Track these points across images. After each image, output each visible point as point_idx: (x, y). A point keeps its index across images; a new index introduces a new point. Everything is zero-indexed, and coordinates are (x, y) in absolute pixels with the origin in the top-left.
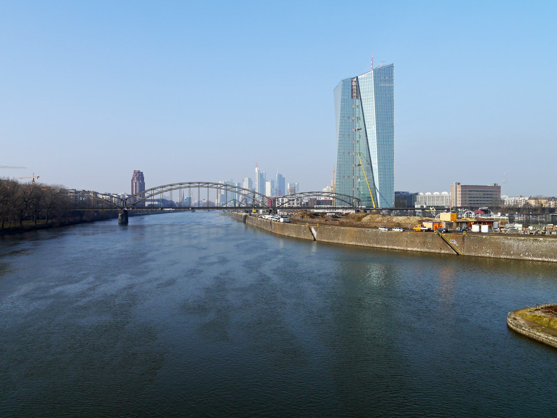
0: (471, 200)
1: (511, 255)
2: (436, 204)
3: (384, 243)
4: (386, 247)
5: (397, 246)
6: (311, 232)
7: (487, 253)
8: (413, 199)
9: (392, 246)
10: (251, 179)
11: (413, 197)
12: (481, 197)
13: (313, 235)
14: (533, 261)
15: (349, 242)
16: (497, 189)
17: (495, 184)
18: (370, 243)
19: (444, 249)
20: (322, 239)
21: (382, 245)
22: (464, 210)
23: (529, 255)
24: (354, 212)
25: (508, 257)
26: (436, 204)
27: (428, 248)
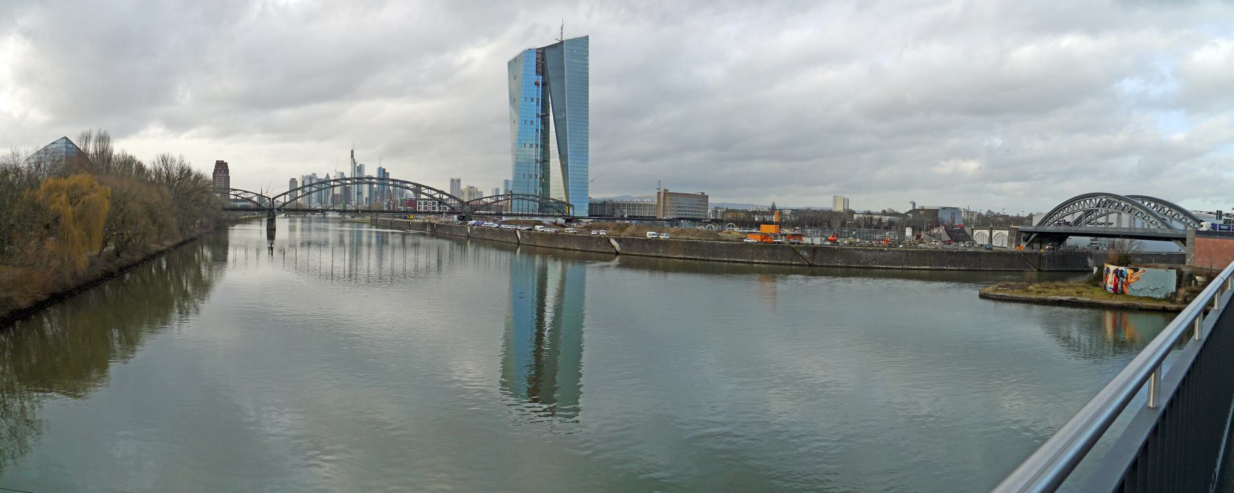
0: (679, 211)
1: (860, 264)
4: (726, 259)
6: (611, 243)
7: (839, 263)
12: (689, 207)
13: (613, 246)
14: (879, 268)
15: (677, 254)
16: (704, 198)
17: (703, 193)
18: (705, 256)
19: (795, 261)
23: (875, 264)
24: (563, 221)
25: (858, 266)
27: (779, 260)
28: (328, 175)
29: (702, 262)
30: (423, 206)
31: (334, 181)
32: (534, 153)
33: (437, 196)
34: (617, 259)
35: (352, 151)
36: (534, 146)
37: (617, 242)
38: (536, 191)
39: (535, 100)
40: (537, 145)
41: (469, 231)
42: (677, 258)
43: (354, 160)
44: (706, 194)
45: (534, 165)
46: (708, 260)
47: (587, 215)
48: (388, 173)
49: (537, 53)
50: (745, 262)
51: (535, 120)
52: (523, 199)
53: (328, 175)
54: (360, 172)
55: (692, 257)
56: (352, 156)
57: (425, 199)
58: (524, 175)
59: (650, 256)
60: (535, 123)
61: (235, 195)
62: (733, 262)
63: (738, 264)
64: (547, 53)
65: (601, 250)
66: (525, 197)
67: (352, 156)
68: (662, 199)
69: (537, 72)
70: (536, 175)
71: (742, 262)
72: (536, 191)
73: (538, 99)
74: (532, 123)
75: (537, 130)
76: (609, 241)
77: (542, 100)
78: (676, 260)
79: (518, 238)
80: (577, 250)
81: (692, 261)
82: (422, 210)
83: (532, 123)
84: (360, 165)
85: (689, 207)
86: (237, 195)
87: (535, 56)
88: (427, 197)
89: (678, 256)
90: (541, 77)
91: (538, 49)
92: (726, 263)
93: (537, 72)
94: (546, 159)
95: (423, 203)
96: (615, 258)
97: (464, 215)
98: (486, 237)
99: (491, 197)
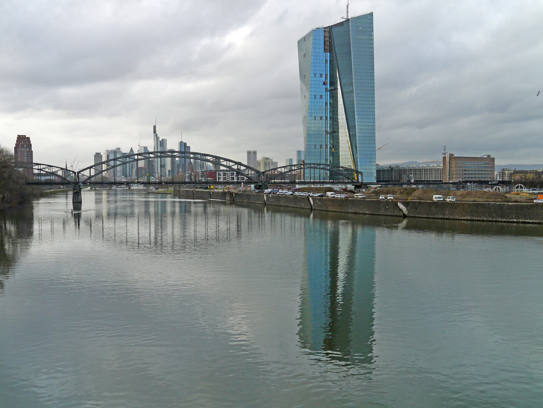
2: (423, 178)
3: (512, 216)
4: (515, 220)
5: (531, 220)
6: (398, 207)
8: (393, 173)
9: (524, 220)
10: (147, 147)
11: (393, 171)
13: (401, 210)
15: (461, 216)
17: (489, 156)
18: (493, 217)
20: (417, 214)
21: (510, 218)
22: (474, 184)
26: (423, 178)
28: (132, 149)
29: (490, 223)
30: (222, 176)
31: (138, 155)
32: (324, 126)
33: (235, 167)
34: (405, 222)
35: (155, 127)
36: (324, 118)
37: (405, 206)
38: (326, 160)
39: (324, 76)
40: (326, 117)
41: (265, 199)
42: (464, 220)
43: (156, 135)
44: (491, 157)
45: (324, 136)
46: (496, 221)
47: (375, 181)
48: (189, 147)
49: (325, 31)
50: (536, 223)
51: (324, 94)
52: (314, 168)
53: (132, 149)
54: (163, 146)
55: (479, 219)
56: (155, 132)
57: (224, 171)
58: (315, 145)
59: (437, 218)
60: (324, 97)
61: (38, 169)
62: (522, 223)
63: (528, 225)
64: (334, 30)
65: (390, 214)
66: (316, 166)
67: (155, 132)
68: (447, 164)
69: (325, 49)
70: (326, 146)
71: (533, 223)
72: (326, 160)
73: (326, 75)
74: (321, 97)
75: (326, 104)
76: (397, 205)
77: (330, 75)
78: (463, 221)
79: (310, 204)
80: (367, 214)
81: (479, 223)
82: (221, 180)
83: (321, 97)
84: (163, 140)
85: (475, 170)
86: (41, 170)
87: (322, 34)
88: (225, 169)
89: (465, 218)
90: (328, 54)
91: (325, 28)
92: (515, 224)
93: (325, 50)
94: (335, 130)
95: (222, 174)
96: (402, 221)
97: (261, 184)
98: (282, 204)
99: (284, 167)
